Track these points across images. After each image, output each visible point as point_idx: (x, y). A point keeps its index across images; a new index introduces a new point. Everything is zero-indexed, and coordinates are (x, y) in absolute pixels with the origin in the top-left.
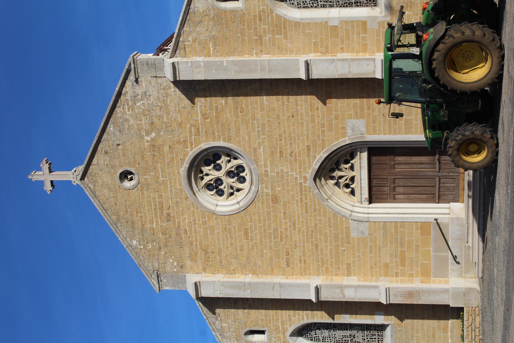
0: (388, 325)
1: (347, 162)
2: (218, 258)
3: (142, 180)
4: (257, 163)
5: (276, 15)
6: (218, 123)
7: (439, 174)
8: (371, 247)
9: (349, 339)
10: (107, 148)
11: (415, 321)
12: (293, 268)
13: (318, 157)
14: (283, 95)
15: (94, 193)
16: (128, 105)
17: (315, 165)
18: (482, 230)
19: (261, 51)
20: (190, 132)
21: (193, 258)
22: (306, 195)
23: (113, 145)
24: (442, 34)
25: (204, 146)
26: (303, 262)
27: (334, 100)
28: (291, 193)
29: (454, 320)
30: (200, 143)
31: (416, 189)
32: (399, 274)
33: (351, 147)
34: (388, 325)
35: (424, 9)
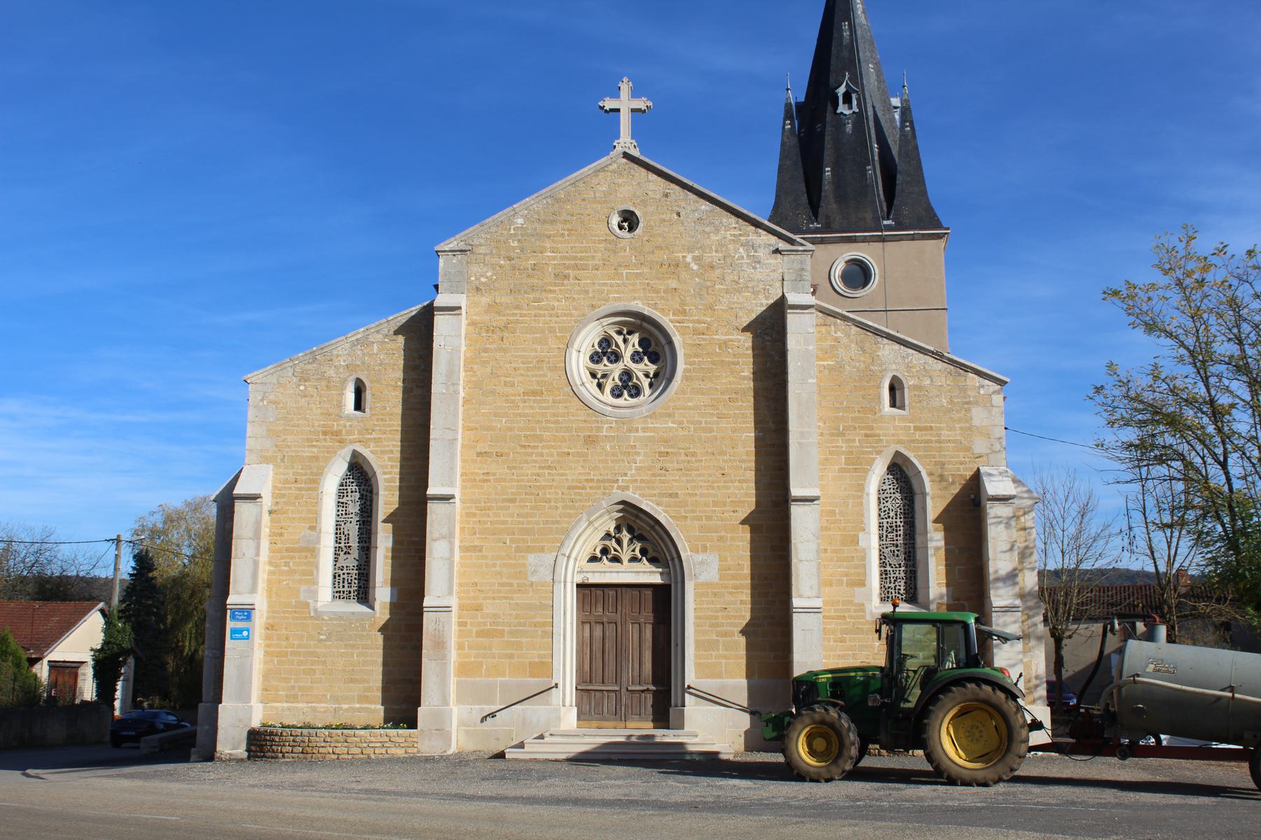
0: (373, 608)
1: (644, 552)
2: (492, 347)
3: (623, 243)
4: (651, 416)
5: (874, 459)
6: (713, 363)
7: (624, 690)
8: (511, 585)
10: (673, 197)
11: (381, 651)
12: (474, 461)
13: (659, 509)
14: (756, 462)
15: (603, 169)
19: (822, 434)
20: (699, 322)
21: (493, 307)
22: (599, 488)
25: (677, 340)
27: (749, 535)
29: (382, 714)
30: (682, 334)
31: (599, 656)
33: (673, 559)
34: (373, 608)
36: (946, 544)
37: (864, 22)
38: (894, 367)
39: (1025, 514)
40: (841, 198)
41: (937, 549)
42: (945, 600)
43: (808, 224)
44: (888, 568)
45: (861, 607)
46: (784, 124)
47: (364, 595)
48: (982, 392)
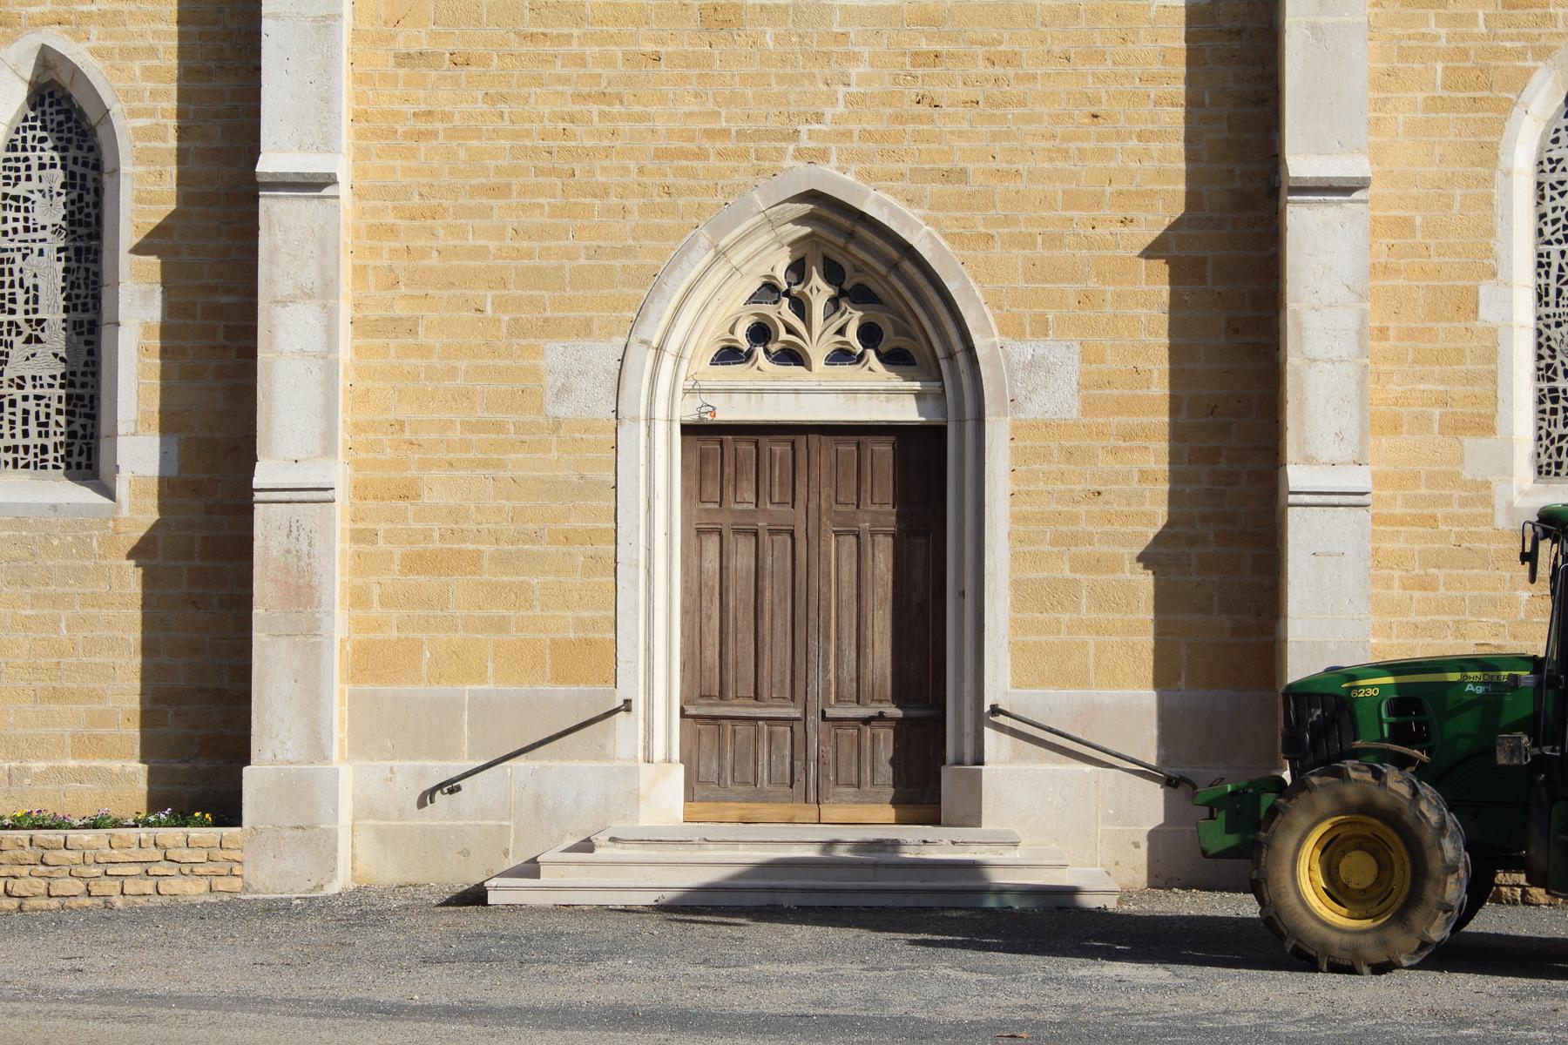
0: (110, 493)
1: (869, 334)
5: (1529, 73)
7: (813, 718)
8: (498, 427)
9: (19, 317)
11: (136, 614)
13: (914, 214)
14: (1190, 80)
17: (881, 203)
18: (447, 903)
22: (743, 155)
26: (423, 126)
27: (1164, 290)
28: (749, 92)
29: (143, 785)
32: (364, 547)
33: (951, 356)
34: (110, 493)
45: (1481, 493)
47: (85, 457)
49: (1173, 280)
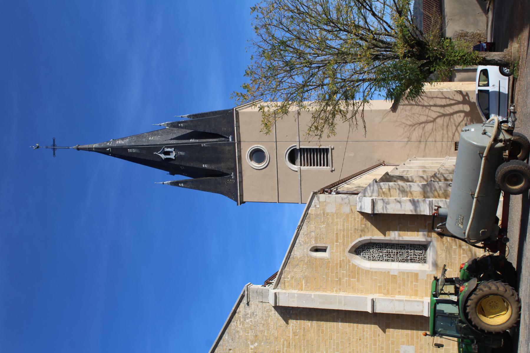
5: (353, 264)
6: (304, 340)
16: (240, 320)
19: (340, 289)
20: (283, 345)
23: (226, 349)
24: (474, 287)
27: (391, 330)
35: (461, 268)
36: (396, 230)
37: (128, 140)
38: (305, 250)
39: (381, 188)
40: (218, 160)
41: (399, 235)
42: (426, 233)
43: (232, 179)
44: (409, 258)
46: (181, 186)
48: (318, 206)
49: (389, 328)
